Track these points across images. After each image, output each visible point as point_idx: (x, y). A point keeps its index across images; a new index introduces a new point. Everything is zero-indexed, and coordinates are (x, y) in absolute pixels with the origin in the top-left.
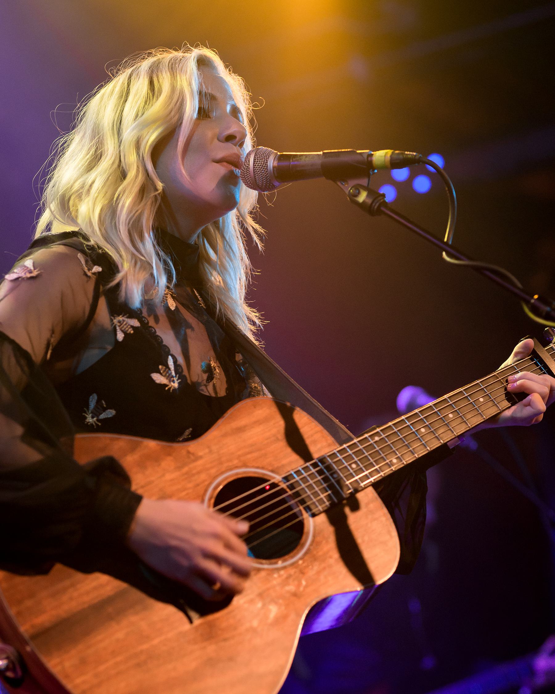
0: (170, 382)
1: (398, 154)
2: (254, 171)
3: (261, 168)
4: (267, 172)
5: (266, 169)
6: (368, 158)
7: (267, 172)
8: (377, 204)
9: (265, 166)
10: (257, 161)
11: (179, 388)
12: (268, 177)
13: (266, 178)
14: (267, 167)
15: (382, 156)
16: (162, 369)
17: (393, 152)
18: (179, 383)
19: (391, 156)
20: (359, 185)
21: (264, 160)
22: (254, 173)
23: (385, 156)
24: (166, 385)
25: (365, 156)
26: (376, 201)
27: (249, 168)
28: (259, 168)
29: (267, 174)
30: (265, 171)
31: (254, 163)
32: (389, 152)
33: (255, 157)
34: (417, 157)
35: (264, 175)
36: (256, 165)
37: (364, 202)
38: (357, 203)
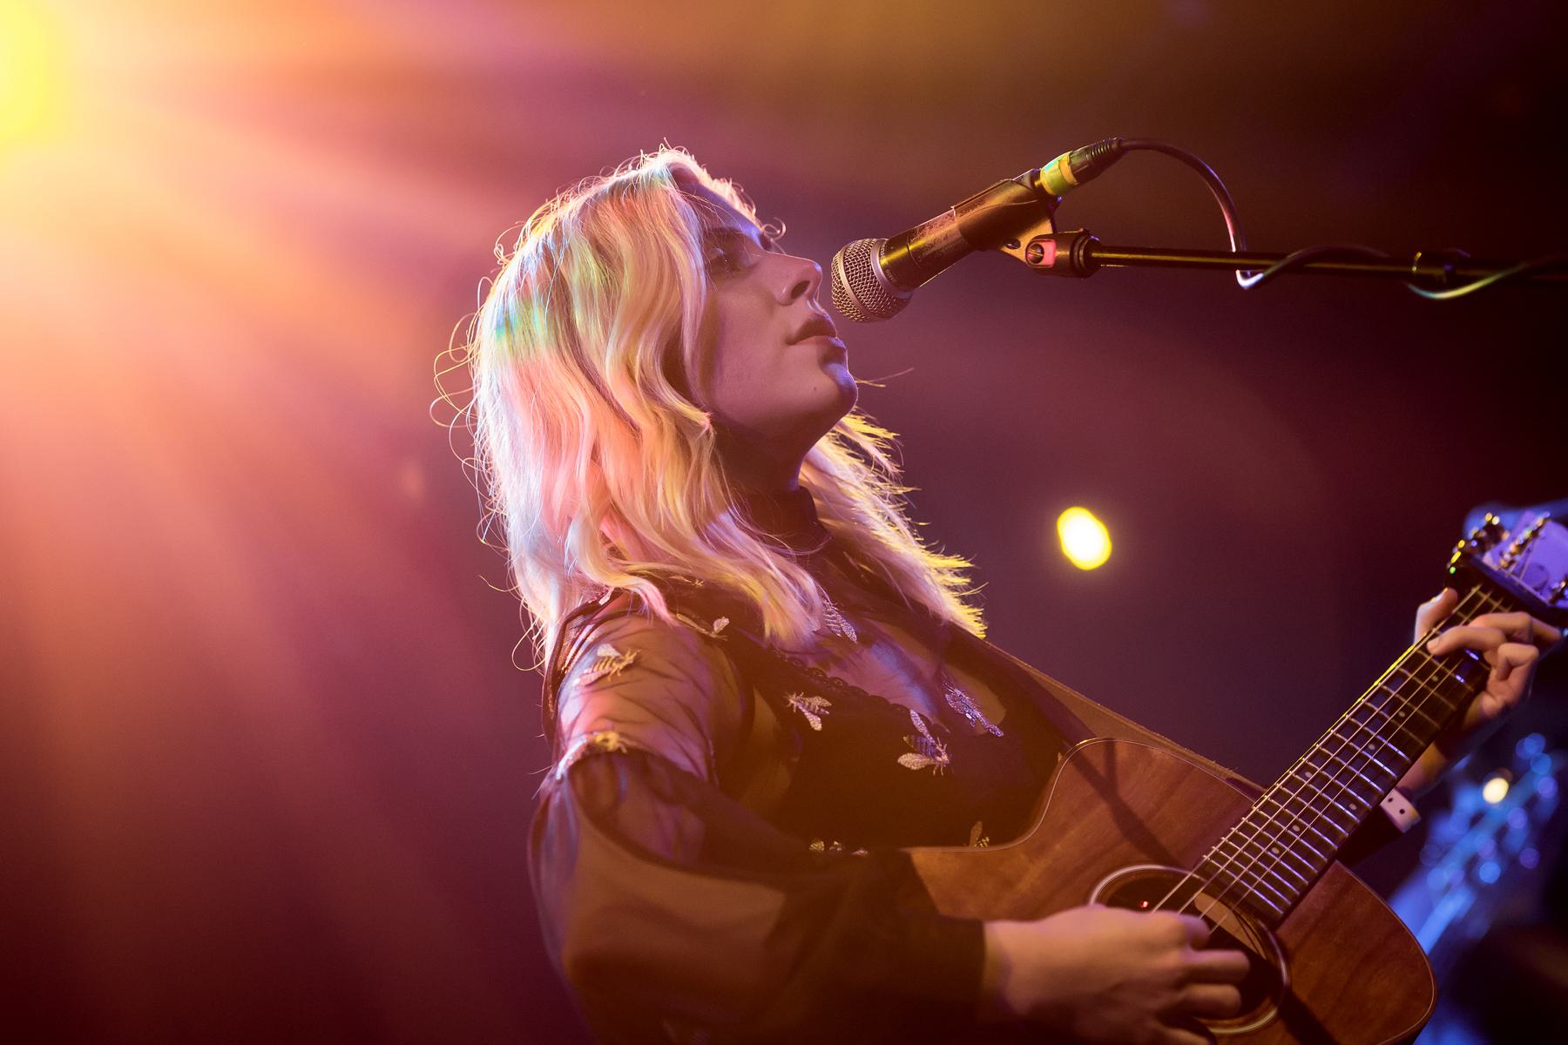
0: (933, 756)
1: (1080, 155)
2: (853, 290)
3: (864, 280)
4: (876, 282)
5: (872, 278)
6: (1032, 182)
7: (876, 282)
8: (1081, 253)
9: (868, 274)
10: (853, 271)
11: (950, 761)
12: (881, 290)
13: (879, 294)
14: (873, 273)
15: (1055, 171)
16: (910, 740)
17: (1071, 154)
18: (947, 752)
19: (1070, 163)
20: (1036, 238)
21: (864, 264)
22: (855, 294)
23: (1059, 168)
24: (929, 767)
25: (1027, 181)
26: (1076, 248)
27: (843, 289)
28: (860, 281)
29: (879, 285)
30: (871, 282)
31: (848, 278)
32: (1065, 157)
33: (845, 266)
34: (1114, 146)
35: (873, 290)
36: (852, 279)
37: (1057, 260)
38: (1046, 271)
